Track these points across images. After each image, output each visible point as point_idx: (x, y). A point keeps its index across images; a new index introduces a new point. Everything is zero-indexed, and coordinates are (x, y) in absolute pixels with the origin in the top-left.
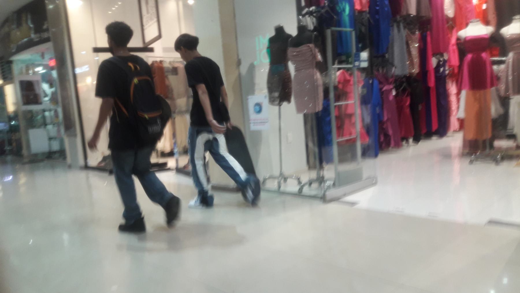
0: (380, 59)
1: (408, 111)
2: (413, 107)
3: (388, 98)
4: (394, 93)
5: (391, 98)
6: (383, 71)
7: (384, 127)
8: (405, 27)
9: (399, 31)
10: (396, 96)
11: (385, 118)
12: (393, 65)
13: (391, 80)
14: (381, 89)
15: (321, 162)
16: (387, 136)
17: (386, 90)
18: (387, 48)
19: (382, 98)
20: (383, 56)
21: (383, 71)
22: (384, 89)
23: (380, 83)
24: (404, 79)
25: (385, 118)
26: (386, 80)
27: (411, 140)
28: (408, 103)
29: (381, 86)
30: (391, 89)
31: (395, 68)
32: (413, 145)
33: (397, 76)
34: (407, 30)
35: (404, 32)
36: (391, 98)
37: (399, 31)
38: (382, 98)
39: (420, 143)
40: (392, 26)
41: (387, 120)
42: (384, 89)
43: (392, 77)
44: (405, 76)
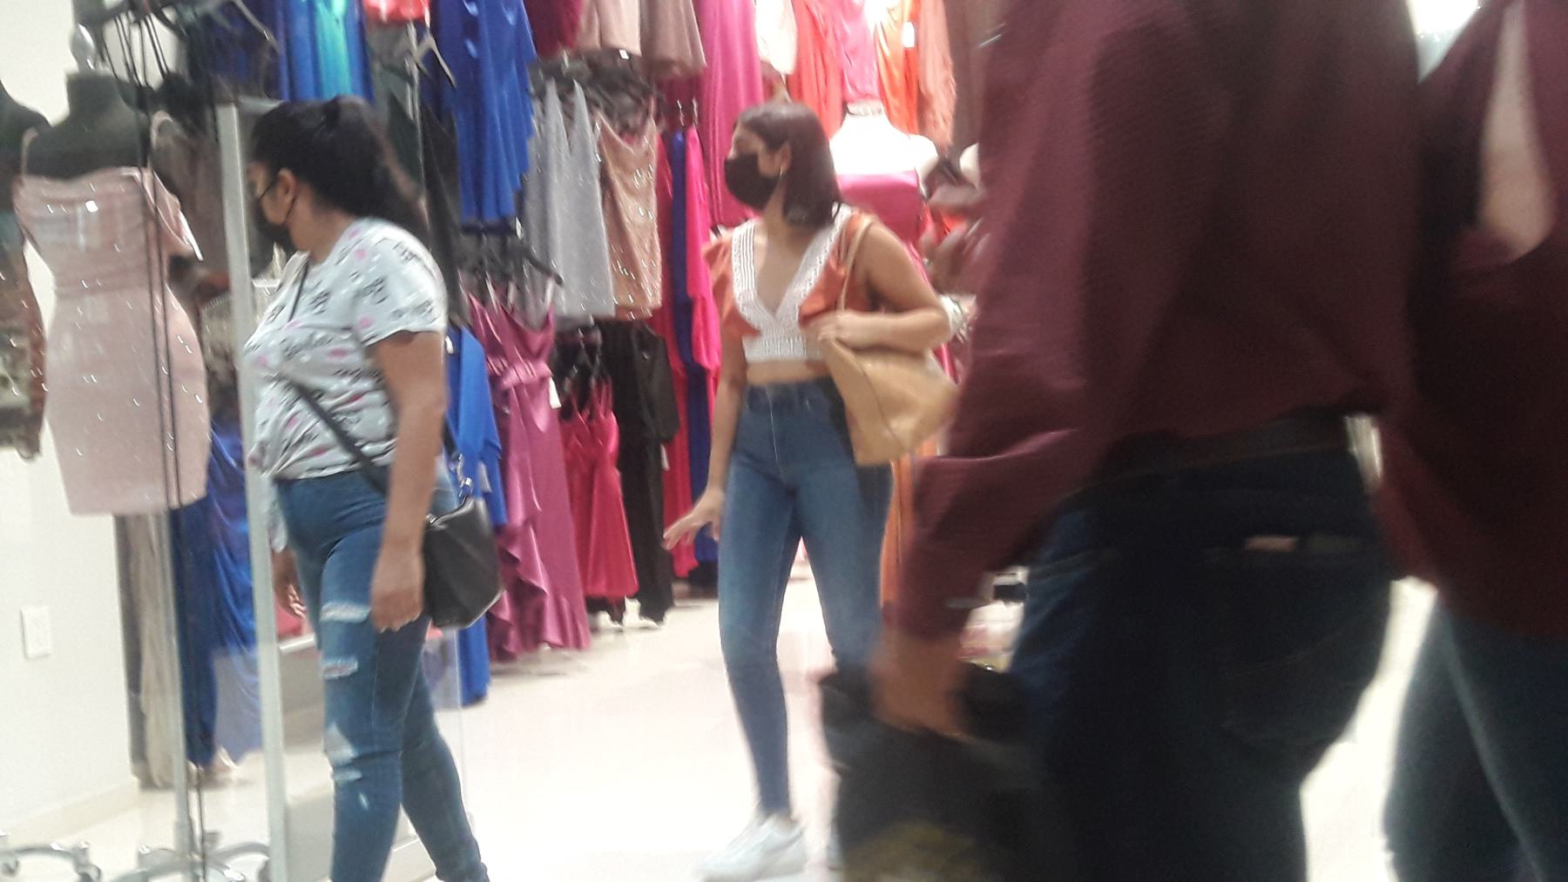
0: (490, 243)
1: (615, 475)
2: (634, 459)
3: (528, 420)
4: (555, 402)
5: (542, 421)
6: (507, 291)
7: (516, 552)
8: (592, 104)
9: (569, 114)
10: (565, 413)
11: (519, 516)
12: (547, 271)
13: (537, 340)
14: (495, 380)
15: (201, 742)
16: (524, 594)
17: (518, 387)
18: (521, 196)
19: (500, 415)
20: (505, 230)
21: (504, 298)
22: (510, 380)
23: (493, 349)
24: (597, 336)
25: (519, 516)
26: (513, 336)
27: (632, 606)
28: (613, 443)
29: (496, 365)
30: (543, 380)
31: (559, 281)
32: (646, 628)
33: (563, 320)
34: (601, 115)
35: (592, 126)
36: (542, 421)
37: (569, 114)
38: (500, 415)
39: (670, 616)
40: (542, 95)
41: (526, 523)
42: (510, 380)
43: (546, 322)
44: (601, 323)
